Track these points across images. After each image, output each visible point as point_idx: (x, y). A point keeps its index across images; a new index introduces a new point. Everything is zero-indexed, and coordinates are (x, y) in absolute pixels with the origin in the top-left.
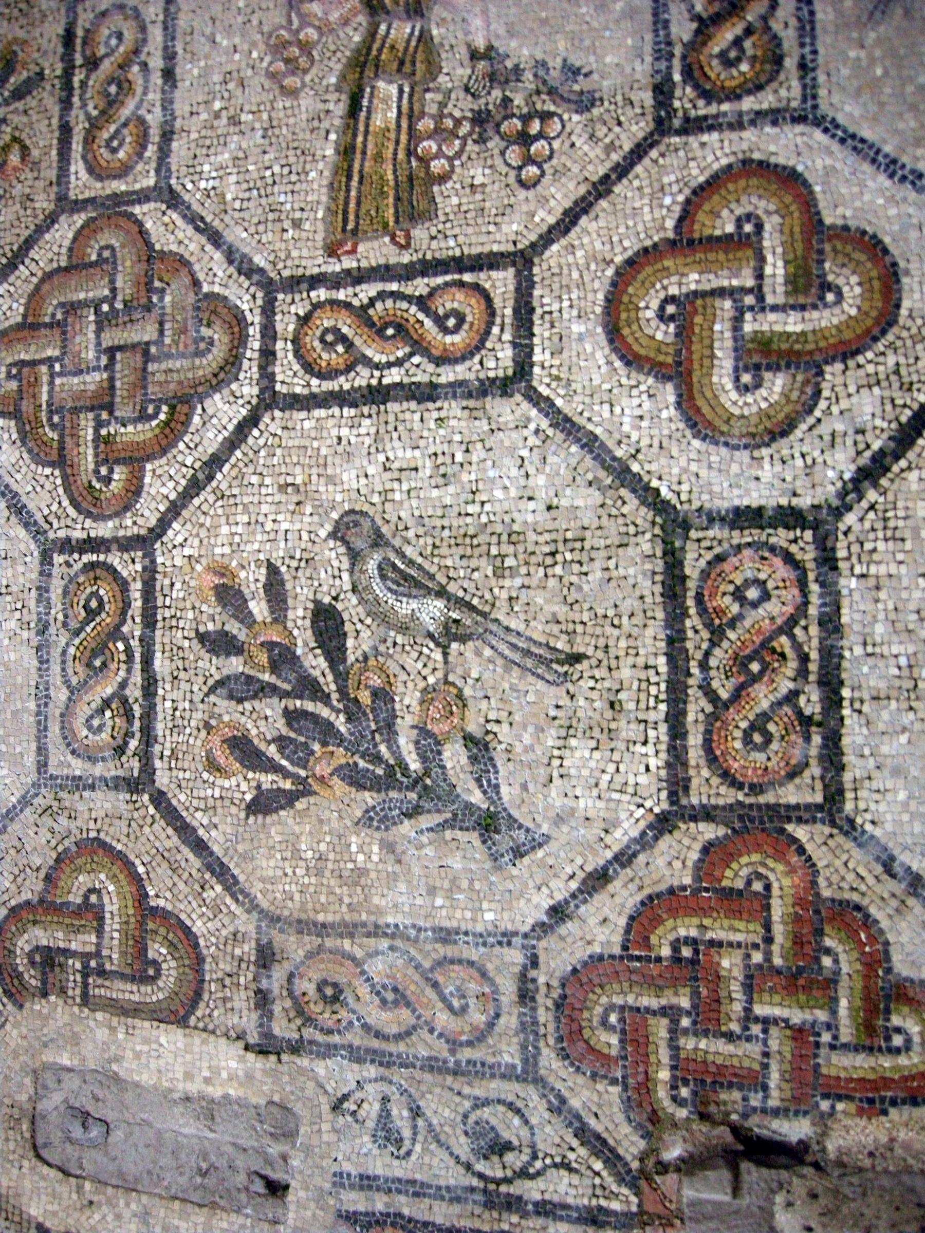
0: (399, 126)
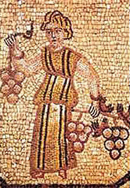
0: (60, 123)
